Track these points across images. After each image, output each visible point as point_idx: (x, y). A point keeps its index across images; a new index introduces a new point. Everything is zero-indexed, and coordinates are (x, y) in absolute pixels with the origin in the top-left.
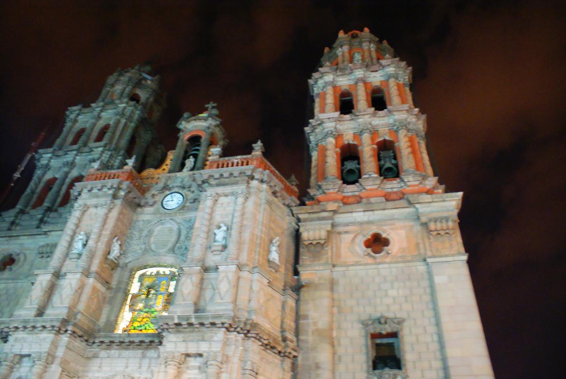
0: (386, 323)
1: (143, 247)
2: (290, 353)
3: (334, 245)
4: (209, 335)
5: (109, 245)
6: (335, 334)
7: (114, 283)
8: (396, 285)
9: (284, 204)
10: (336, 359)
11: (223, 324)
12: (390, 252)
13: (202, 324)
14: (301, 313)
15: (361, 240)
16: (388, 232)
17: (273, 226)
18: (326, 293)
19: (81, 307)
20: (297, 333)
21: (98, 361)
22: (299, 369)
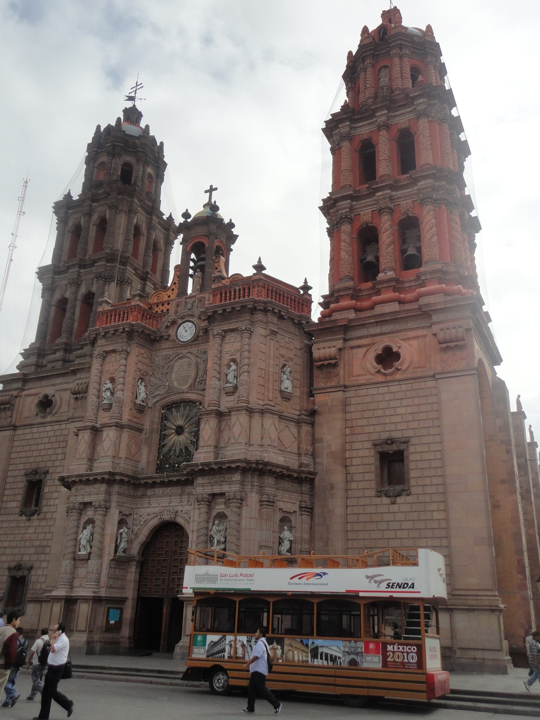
0: (392, 443)
2: (306, 477)
3: (346, 363)
4: (228, 476)
5: (135, 387)
6: (348, 454)
7: (147, 426)
8: (405, 402)
9: (294, 323)
10: (348, 479)
11: (238, 467)
12: (399, 367)
13: (220, 468)
14: (316, 437)
16: (398, 345)
17: (283, 351)
18: (339, 415)
19: (123, 454)
20: (314, 455)
21: (146, 500)
22: (316, 490)
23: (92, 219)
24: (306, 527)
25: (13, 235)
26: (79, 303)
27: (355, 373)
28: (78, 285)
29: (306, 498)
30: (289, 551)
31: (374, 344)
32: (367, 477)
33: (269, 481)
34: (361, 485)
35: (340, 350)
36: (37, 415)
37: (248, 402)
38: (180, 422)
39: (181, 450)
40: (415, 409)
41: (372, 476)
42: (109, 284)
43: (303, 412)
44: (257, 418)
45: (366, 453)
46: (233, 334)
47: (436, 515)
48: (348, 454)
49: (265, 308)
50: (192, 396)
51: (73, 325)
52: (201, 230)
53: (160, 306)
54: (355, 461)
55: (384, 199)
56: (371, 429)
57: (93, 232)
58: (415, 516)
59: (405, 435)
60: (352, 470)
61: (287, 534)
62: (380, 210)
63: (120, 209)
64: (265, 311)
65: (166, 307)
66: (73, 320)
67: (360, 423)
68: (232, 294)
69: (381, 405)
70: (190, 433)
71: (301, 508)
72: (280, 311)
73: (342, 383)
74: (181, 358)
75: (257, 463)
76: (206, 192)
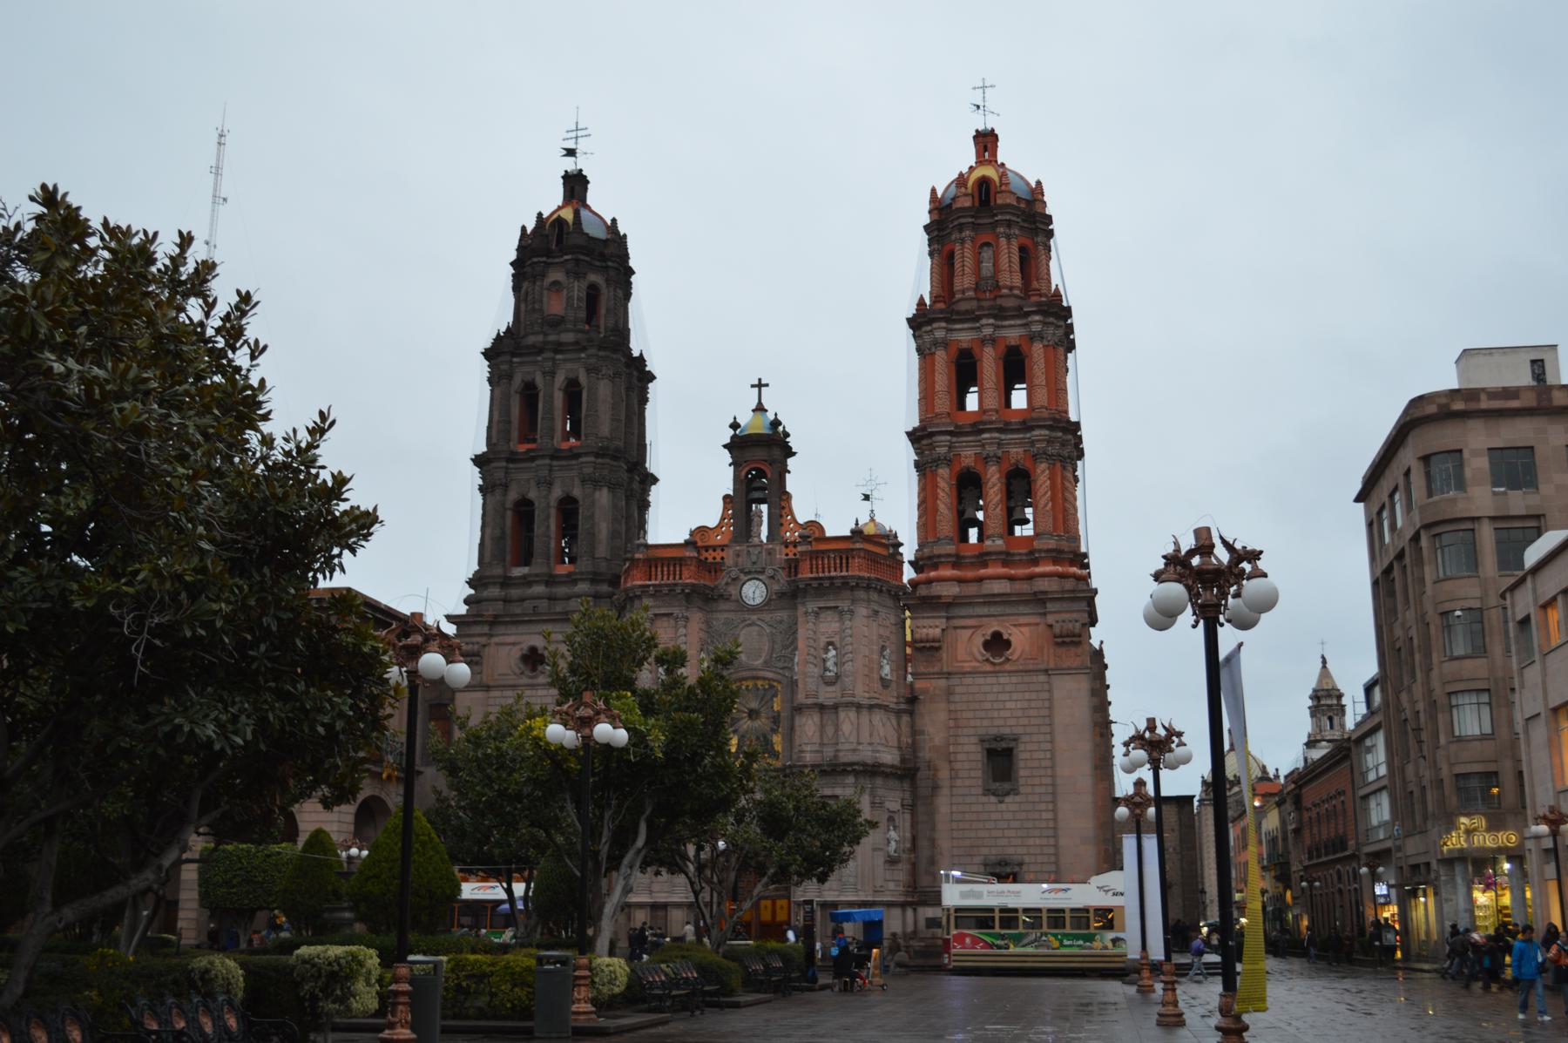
0: (1002, 740)
8: (1015, 696)
9: (890, 594)
11: (854, 770)
15: (979, 640)
17: (882, 631)
23: (556, 380)
24: (908, 824)
25: (207, 243)
26: (553, 512)
27: (959, 658)
28: (550, 484)
29: (907, 795)
30: (895, 852)
31: (980, 627)
32: (973, 774)
33: (879, 781)
34: (967, 782)
36: (522, 673)
37: (853, 696)
38: (754, 705)
39: (758, 739)
40: (1026, 705)
41: (979, 773)
42: (600, 490)
43: (902, 700)
44: (865, 712)
45: (973, 748)
46: (829, 612)
47: (1044, 816)
48: (952, 749)
49: (868, 585)
51: (549, 543)
52: (760, 453)
53: (711, 551)
54: (960, 757)
55: (992, 443)
56: (978, 723)
57: (559, 399)
58: (1024, 815)
59: (1015, 732)
60: (958, 766)
61: (893, 834)
62: (986, 458)
63: (604, 372)
64: (868, 588)
65: (718, 554)
66: (549, 537)
67: (966, 715)
69: (990, 697)
70: (768, 718)
71: (903, 805)
73: (945, 670)
75: (873, 766)
76: (753, 386)
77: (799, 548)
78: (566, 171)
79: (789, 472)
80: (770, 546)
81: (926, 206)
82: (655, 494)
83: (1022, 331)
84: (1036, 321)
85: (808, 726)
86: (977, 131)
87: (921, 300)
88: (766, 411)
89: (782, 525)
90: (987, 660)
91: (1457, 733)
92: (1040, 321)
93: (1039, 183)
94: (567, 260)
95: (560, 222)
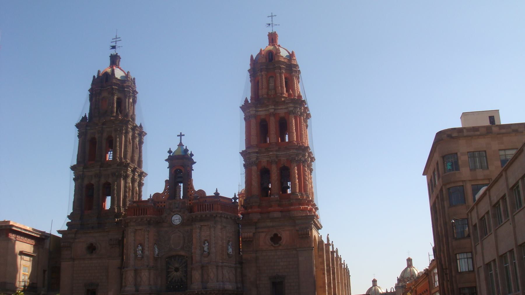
1: (168, 246)
35: (254, 233)
38: (177, 265)
50: (182, 253)
53: (160, 203)
68: (204, 207)
72: (227, 216)
74: (174, 233)
76: (178, 136)
77: (193, 201)
78: (111, 54)
79: (193, 170)
80: (183, 201)
81: (249, 62)
82: (145, 180)
83: (286, 111)
84: (291, 106)
85: (196, 275)
86: (269, 33)
87: (246, 99)
88: (183, 146)
89: (188, 192)
90: (272, 245)
91: (459, 271)
92: (293, 107)
93: (293, 52)
94: (108, 88)
95: (106, 74)
